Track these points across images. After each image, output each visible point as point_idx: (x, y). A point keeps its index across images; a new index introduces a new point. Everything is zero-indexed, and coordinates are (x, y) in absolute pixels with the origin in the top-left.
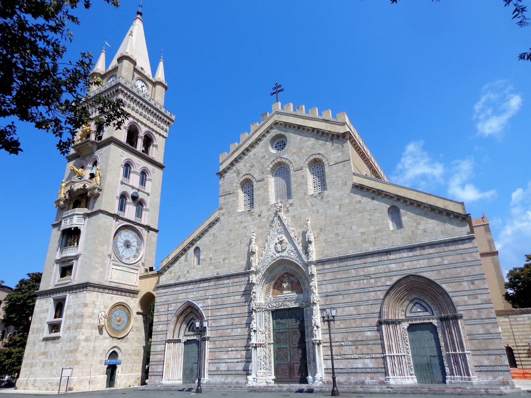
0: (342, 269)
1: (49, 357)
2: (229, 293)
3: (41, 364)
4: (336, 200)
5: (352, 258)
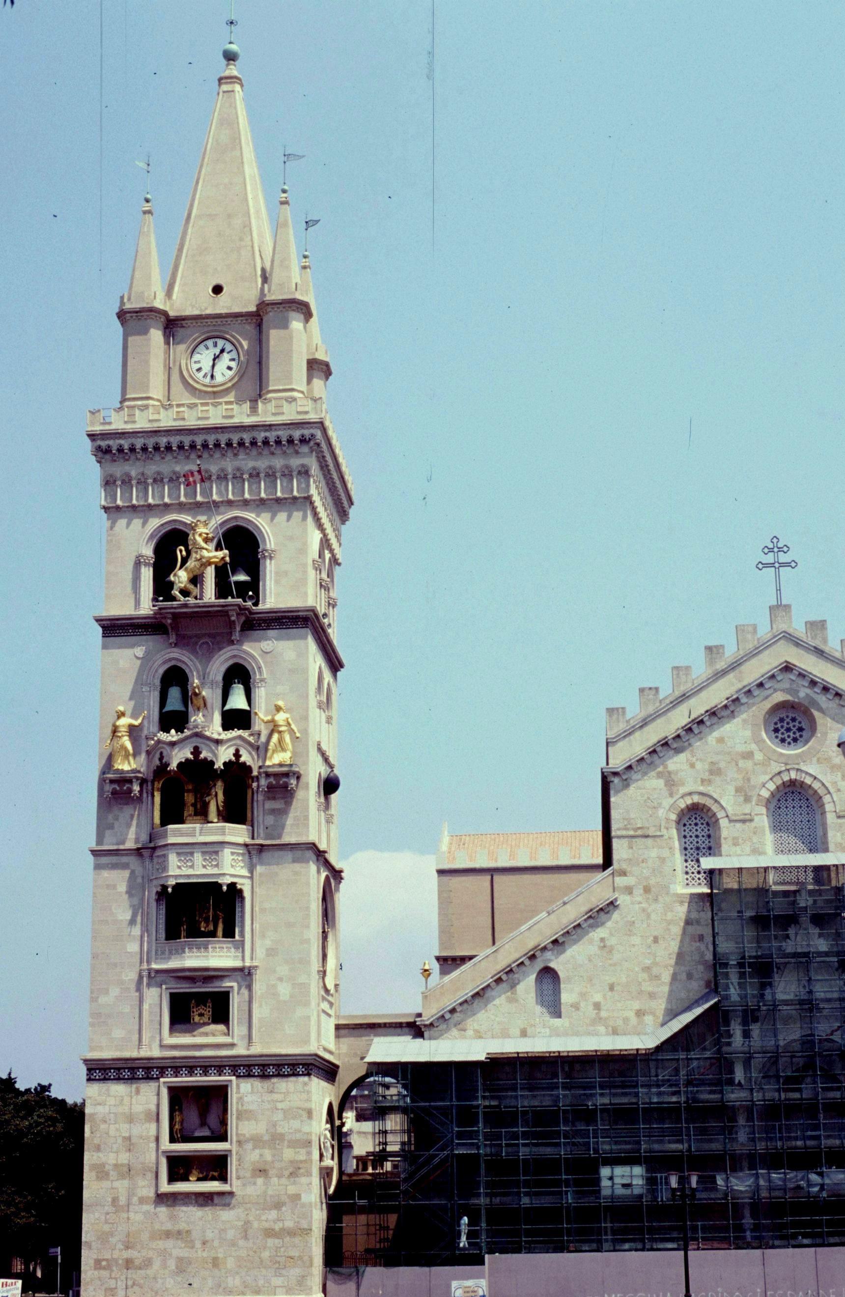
1: (198, 1244)
3: (172, 1264)
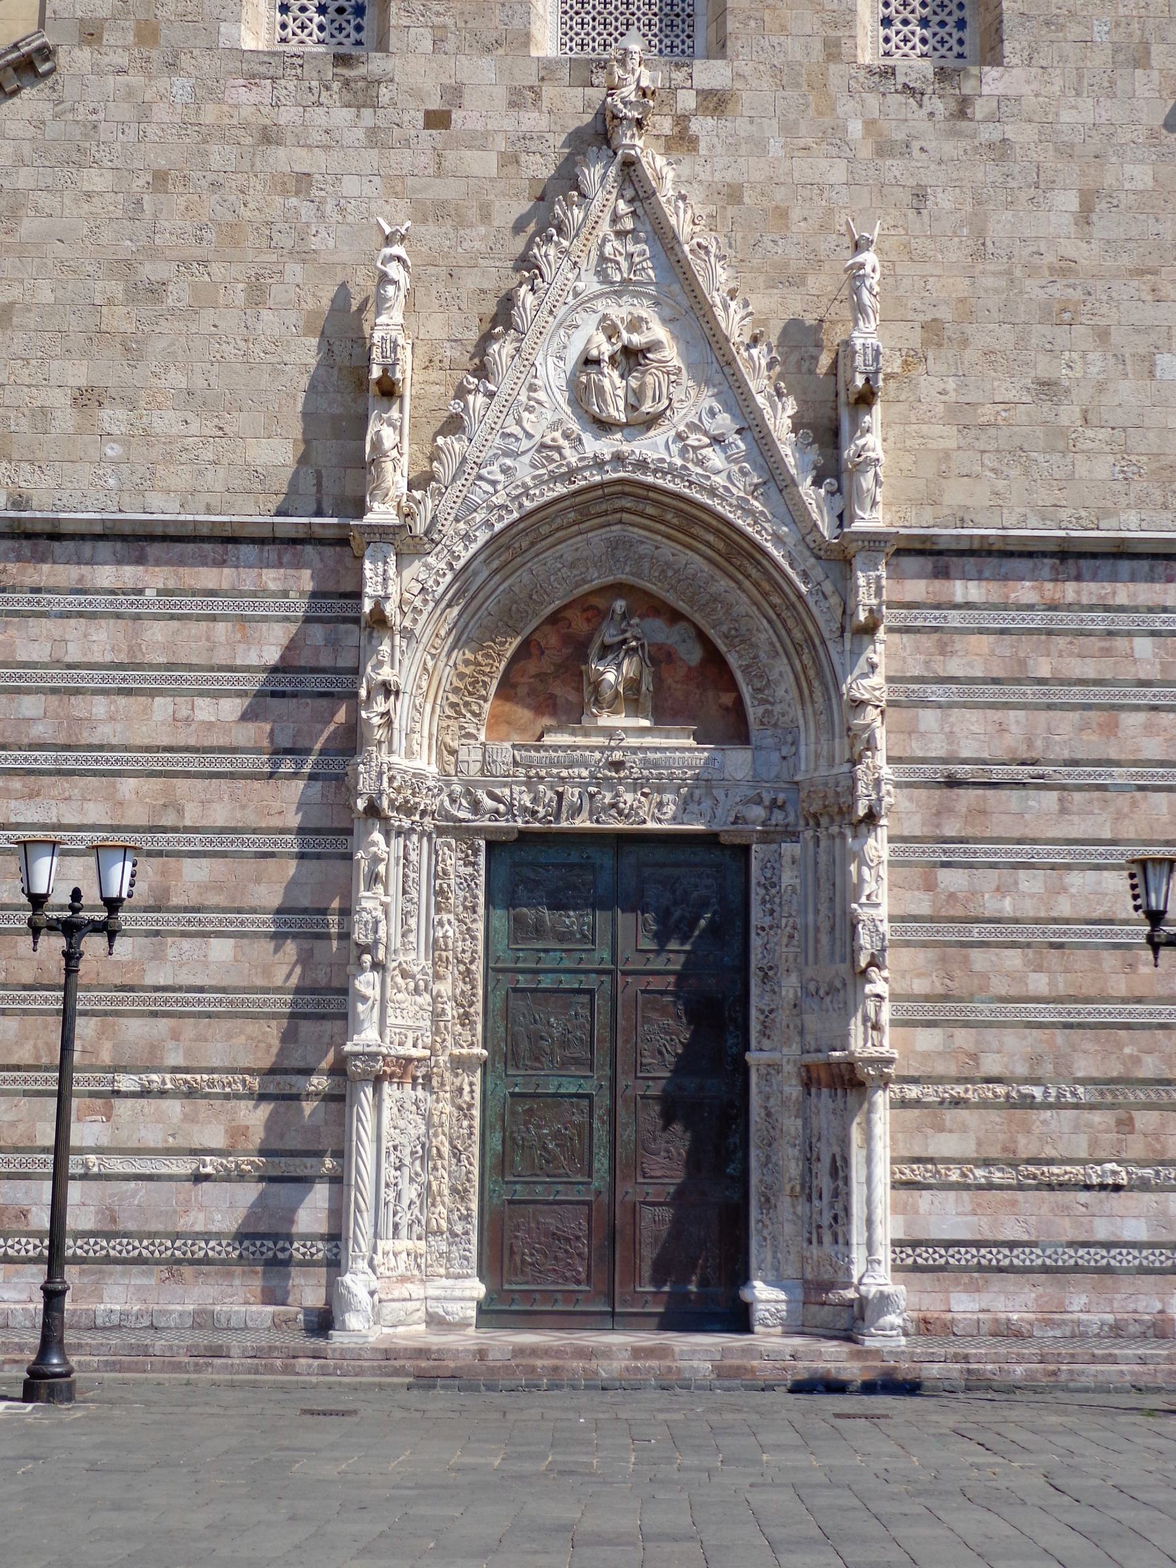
0: (1069, 620)
2: (139, 666)
4: (1066, 151)
5: (1145, 565)
